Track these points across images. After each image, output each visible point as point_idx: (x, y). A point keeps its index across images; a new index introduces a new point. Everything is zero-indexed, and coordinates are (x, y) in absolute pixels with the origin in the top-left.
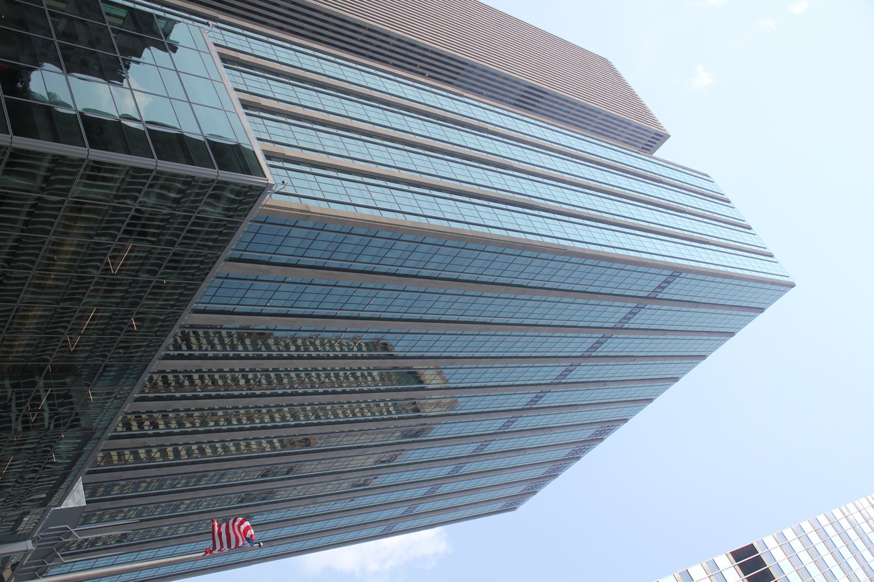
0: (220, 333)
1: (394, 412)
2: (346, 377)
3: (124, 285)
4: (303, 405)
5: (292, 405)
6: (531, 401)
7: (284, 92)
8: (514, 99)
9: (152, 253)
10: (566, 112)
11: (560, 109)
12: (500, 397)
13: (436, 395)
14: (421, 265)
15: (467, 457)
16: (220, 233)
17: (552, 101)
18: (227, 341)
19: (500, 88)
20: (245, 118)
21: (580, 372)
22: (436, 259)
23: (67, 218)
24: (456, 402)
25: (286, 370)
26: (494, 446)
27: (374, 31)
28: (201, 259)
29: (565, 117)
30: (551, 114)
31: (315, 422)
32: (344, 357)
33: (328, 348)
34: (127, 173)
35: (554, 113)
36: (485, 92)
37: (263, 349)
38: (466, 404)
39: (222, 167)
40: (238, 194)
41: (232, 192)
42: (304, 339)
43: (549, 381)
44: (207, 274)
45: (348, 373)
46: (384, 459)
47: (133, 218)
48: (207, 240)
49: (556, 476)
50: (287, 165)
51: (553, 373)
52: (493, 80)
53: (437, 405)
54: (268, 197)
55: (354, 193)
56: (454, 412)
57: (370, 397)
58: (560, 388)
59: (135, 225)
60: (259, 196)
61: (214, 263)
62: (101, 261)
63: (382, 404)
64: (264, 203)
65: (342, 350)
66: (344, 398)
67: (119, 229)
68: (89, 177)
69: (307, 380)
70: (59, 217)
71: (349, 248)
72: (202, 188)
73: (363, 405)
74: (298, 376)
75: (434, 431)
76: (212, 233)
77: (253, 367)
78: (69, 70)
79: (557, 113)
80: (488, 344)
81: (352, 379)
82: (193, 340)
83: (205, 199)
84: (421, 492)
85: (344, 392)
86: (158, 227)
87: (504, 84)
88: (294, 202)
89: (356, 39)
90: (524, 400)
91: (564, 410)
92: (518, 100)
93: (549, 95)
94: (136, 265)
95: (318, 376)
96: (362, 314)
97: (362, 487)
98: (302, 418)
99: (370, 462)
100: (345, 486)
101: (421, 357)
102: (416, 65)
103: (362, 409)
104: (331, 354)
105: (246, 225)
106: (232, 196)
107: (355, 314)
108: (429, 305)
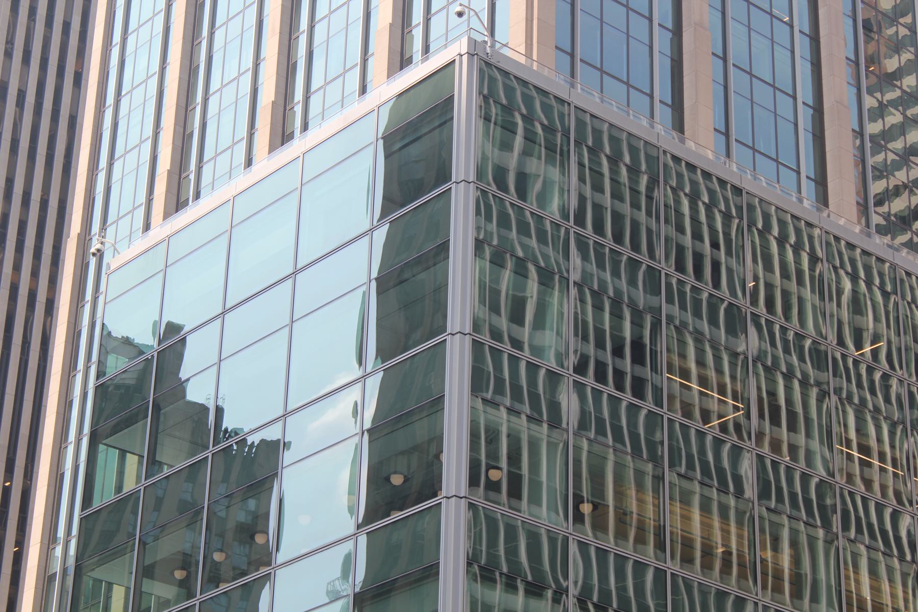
0: (872, 137)
3: (771, 381)
7: (234, 47)
9: (684, 324)
16: (614, 161)
18: (894, 118)
20: (315, 134)
23: (621, 534)
28: (685, 203)
34: (495, 405)
37: (908, 19)
39: (443, 175)
40: (509, 128)
41: (506, 146)
44: (722, 183)
47: (601, 377)
48: (635, 192)
54: (506, 51)
59: (619, 375)
60: (506, 74)
61: (691, 167)
62: (718, 443)
64: (522, 60)
67: (633, 410)
68: (515, 492)
70: (621, 551)
72: (504, 221)
76: (614, 181)
78: (264, 558)
82: (898, 205)
83: (532, 205)
86: (617, 315)
94: (718, 359)
105: (585, 95)
106: (519, 141)
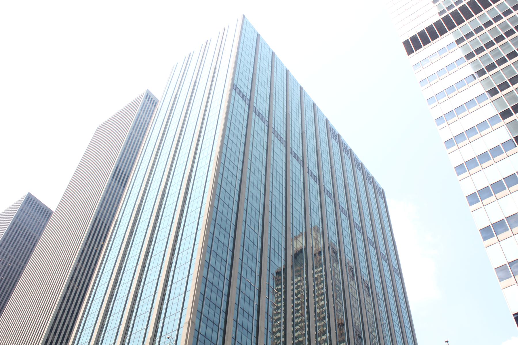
1: (321, 268)
2: (298, 299)
4: (316, 327)
5: (316, 335)
6: (314, 179)
7: (110, 338)
8: (120, 187)
10: (130, 154)
11: (128, 158)
12: (312, 199)
13: (310, 240)
14: (225, 248)
15: (350, 221)
17: (123, 163)
21: (296, 148)
22: (222, 238)
24: (314, 228)
25: (293, 339)
26: (343, 203)
27: (72, 277)
29: (133, 155)
30: (131, 164)
31: (327, 319)
32: (285, 300)
33: (279, 311)
35: (130, 162)
36: (115, 206)
38: (315, 221)
42: (273, 326)
43: (302, 168)
45: (295, 297)
46: (351, 275)
49: (362, 164)
50: (158, 336)
51: (297, 165)
52: (108, 200)
53: (316, 239)
55: (178, 291)
56: (321, 229)
57: (311, 284)
58: (306, 161)
63: (316, 276)
65: (280, 302)
66: (312, 301)
69: (300, 325)
71: (214, 296)
73: (316, 288)
74: (297, 331)
75: (333, 241)
77: (291, 301)
79: (131, 160)
80: (277, 206)
81: (299, 296)
84: (372, 250)
85: (308, 300)
87: (110, 193)
88: (183, 331)
89: (77, 289)
90: (313, 184)
91: (320, 159)
92: (121, 185)
93: (118, 165)
95: (298, 317)
96: (257, 288)
97: (369, 288)
98: (325, 328)
99: (354, 284)
100: (369, 300)
101: (286, 249)
102: (96, 250)
103: (319, 289)
104: (283, 309)
107: (257, 292)
108: (251, 244)
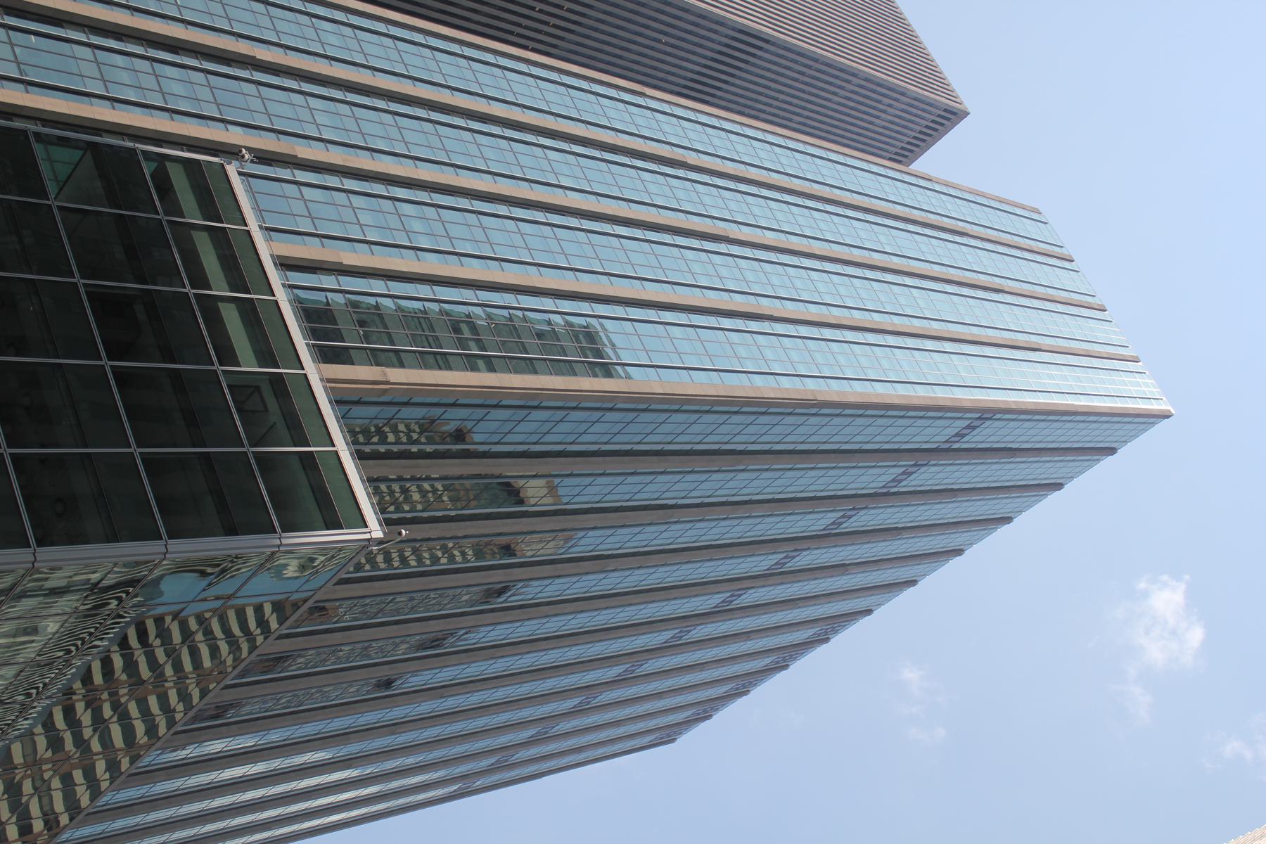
8: (712, 50)
19: (690, 33)
87: (697, 25)
92: (720, 53)
93: (774, 44)
